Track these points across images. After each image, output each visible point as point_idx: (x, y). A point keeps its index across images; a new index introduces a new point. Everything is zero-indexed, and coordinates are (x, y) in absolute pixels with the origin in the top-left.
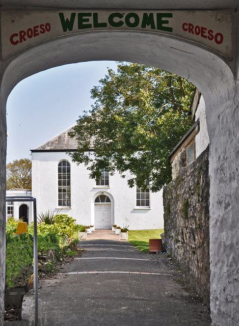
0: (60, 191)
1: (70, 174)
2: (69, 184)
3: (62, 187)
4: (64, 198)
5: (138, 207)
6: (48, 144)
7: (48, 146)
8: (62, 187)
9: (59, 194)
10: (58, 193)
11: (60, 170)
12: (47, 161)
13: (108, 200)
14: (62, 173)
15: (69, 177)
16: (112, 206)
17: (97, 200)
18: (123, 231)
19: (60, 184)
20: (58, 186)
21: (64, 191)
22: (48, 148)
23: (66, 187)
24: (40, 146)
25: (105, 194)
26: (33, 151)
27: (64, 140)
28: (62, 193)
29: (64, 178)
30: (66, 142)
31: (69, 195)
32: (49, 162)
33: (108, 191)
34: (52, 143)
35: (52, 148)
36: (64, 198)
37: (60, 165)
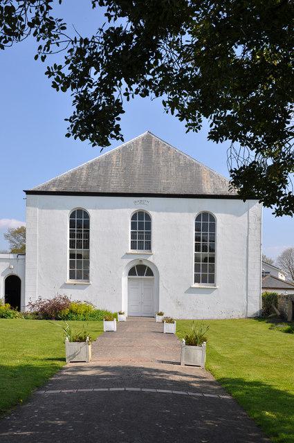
0: (72, 256)
1: (88, 231)
2: (87, 245)
3: (76, 251)
4: (79, 266)
5: (197, 285)
6: (53, 183)
7: (54, 185)
8: (76, 251)
9: (70, 261)
10: (68, 259)
11: (72, 224)
12: (52, 209)
13: (150, 273)
14: (76, 229)
15: (87, 236)
16: (155, 282)
17: (132, 272)
18: (140, 270)
19: (72, 246)
20: (68, 248)
21: (79, 256)
22: (54, 189)
23: (82, 251)
24: (40, 185)
25: (145, 263)
26: (28, 193)
27: (80, 179)
28: (76, 260)
29: (79, 236)
30: (83, 182)
31: (87, 264)
32: (54, 211)
33: (150, 259)
34: (61, 181)
35: (61, 189)
36: (79, 266)
37: (72, 216)
